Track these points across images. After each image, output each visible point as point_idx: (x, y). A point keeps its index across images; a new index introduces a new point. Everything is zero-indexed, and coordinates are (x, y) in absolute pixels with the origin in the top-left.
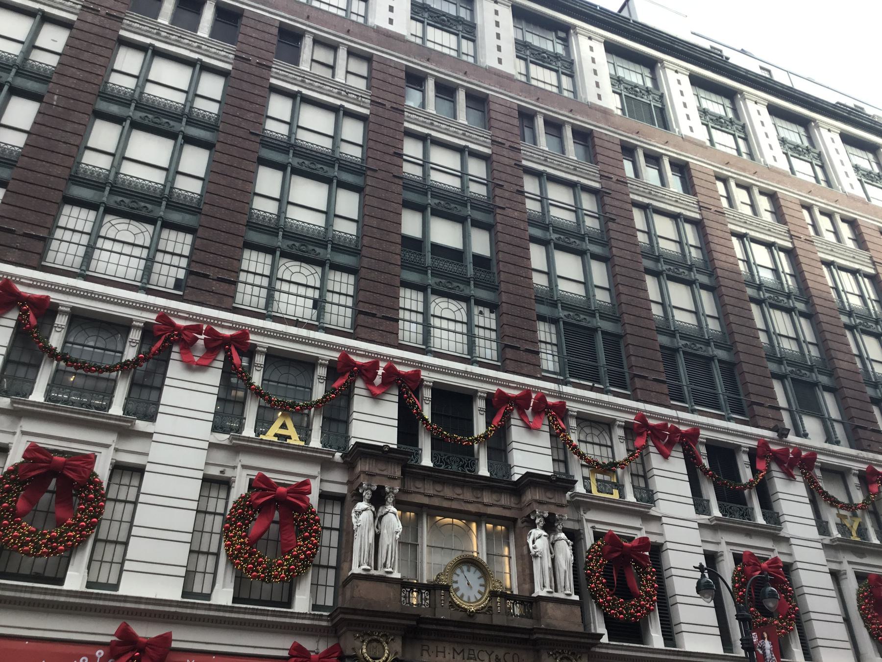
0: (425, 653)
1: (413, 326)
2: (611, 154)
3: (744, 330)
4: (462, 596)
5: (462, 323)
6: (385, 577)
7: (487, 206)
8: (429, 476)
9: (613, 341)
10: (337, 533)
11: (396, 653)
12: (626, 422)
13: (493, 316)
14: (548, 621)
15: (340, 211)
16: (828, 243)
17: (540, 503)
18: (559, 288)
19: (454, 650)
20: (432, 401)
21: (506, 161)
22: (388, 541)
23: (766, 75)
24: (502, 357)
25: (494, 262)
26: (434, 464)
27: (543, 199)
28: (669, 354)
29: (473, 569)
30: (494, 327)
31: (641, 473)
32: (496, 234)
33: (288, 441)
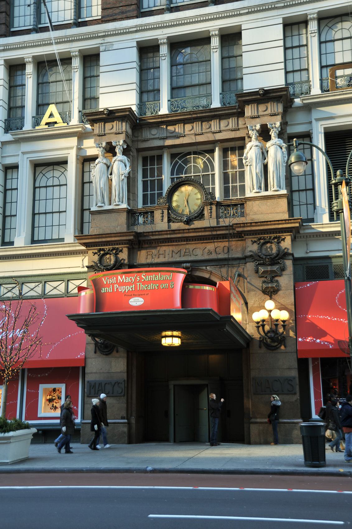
33: (56, 125)
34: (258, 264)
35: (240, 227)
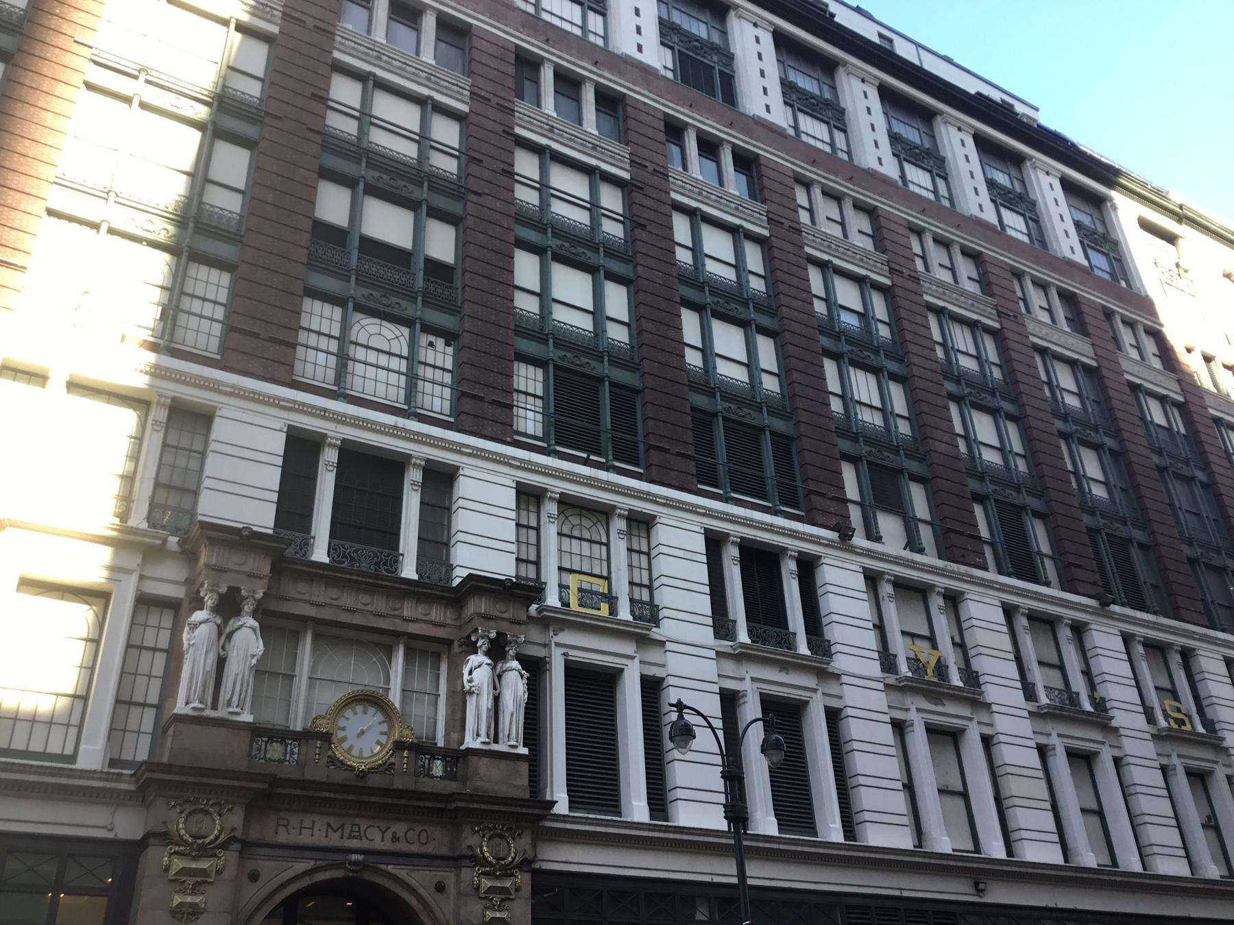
0: (281, 830)
1: (322, 356)
2: (650, 133)
3: (810, 392)
4: (351, 748)
5: (400, 357)
6: (227, 720)
7: (454, 189)
8: (322, 576)
9: (625, 398)
10: (164, 655)
11: (234, 829)
12: (630, 510)
13: (450, 350)
14: (479, 784)
15: (215, 174)
16: (940, 284)
17: (486, 617)
18: (554, 317)
19: (329, 825)
20: (338, 468)
21: (490, 125)
22: (237, 667)
23: (886, 45)
24: (456, 410)
25: (459, 271)
26: (333, 560)
27: (543, 187)
28: (703, 420)
29: (371, 710)
30: (449, 366)
31: (646, 582)
32: (464, 232)
34: (174, 853)
35: (464, 801)
